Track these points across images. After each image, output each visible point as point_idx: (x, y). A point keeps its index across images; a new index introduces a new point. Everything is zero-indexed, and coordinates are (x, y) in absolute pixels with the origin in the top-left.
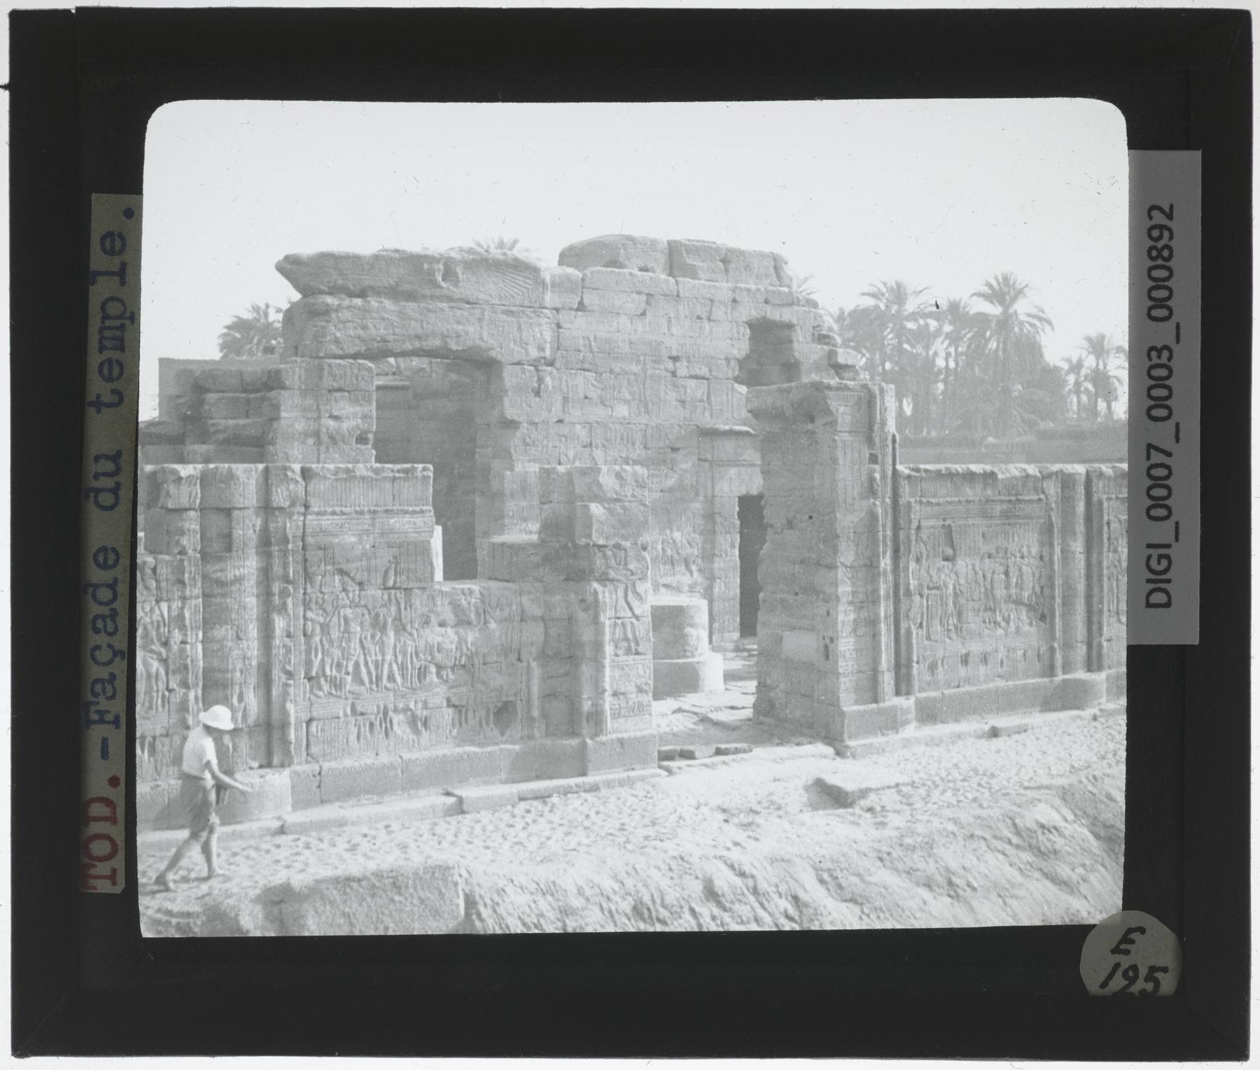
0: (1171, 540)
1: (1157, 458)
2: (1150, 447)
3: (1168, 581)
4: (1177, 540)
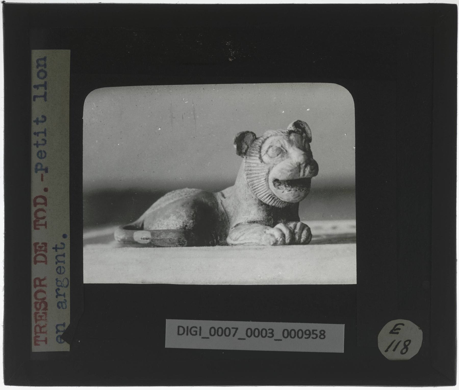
0: (203, 335)
1: (233, 331)
2: (237, 329)
3: (187, 334)
4: (202, 338)
